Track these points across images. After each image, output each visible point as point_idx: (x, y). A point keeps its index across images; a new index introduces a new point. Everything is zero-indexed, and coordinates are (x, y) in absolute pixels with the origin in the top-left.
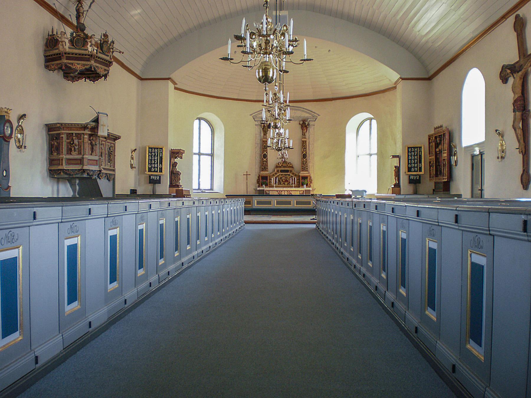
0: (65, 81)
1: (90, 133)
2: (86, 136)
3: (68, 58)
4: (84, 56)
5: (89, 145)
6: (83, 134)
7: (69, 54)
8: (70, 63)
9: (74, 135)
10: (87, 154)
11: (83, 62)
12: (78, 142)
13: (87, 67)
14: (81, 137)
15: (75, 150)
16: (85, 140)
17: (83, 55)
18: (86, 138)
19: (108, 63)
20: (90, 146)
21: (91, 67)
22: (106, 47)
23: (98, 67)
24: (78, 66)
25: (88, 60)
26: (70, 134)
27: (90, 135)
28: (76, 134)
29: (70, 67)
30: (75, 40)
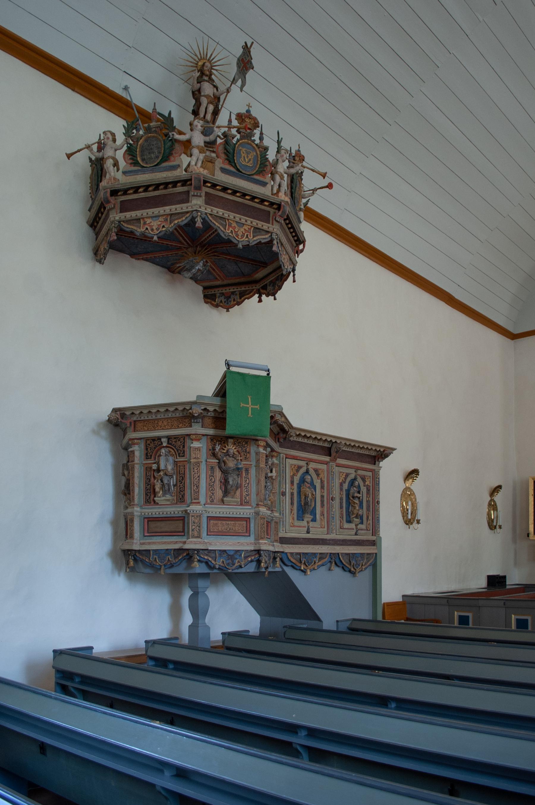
0: (206, 308)
1: (211, 432)
2: (196, 444)
3: (125, 207)
4: (171, 190)
5: (212, 468)
6: (189, 435)
7: (125, 192)
8: (128, 222)
9: (165, 444)
10: (202, 499)
11: (167, 209)
12: (176, 463)
13: (183, 221)
14: (184, 447)
15: (166, 490)
16: (193, 456)
17: (166, 185)
18: (198, 449)
19: (272, 211)
20: (218, 474)
21: (193, 221)
22: (248, 153)
23: (223, 219)
24: (155, 224)
25: (185, 198)
26: (153, 439)
27: (213, 439)
28: (169, 438)
29: (132, 232)
30: (142, 146)
